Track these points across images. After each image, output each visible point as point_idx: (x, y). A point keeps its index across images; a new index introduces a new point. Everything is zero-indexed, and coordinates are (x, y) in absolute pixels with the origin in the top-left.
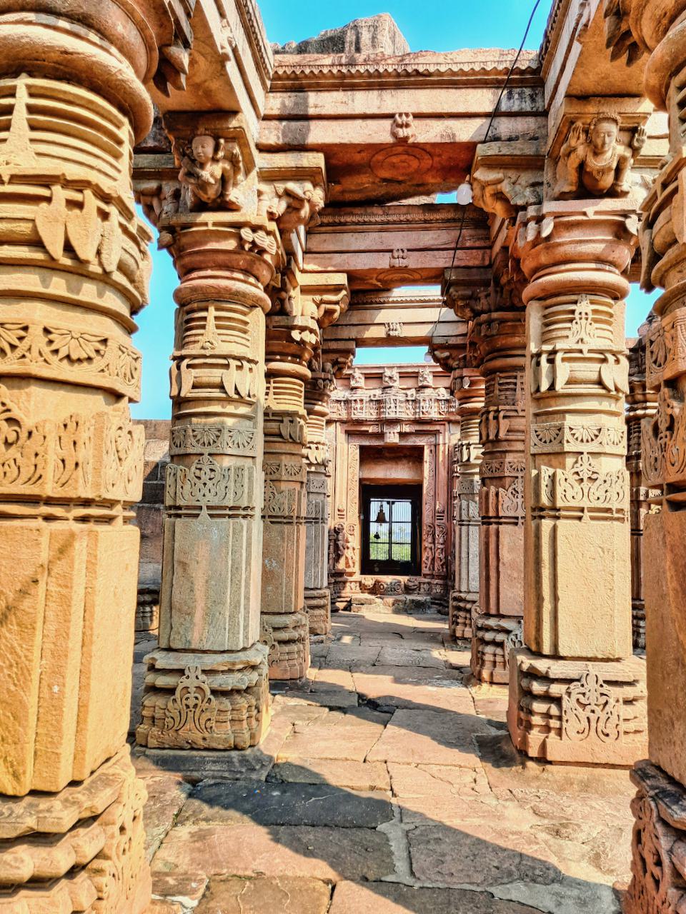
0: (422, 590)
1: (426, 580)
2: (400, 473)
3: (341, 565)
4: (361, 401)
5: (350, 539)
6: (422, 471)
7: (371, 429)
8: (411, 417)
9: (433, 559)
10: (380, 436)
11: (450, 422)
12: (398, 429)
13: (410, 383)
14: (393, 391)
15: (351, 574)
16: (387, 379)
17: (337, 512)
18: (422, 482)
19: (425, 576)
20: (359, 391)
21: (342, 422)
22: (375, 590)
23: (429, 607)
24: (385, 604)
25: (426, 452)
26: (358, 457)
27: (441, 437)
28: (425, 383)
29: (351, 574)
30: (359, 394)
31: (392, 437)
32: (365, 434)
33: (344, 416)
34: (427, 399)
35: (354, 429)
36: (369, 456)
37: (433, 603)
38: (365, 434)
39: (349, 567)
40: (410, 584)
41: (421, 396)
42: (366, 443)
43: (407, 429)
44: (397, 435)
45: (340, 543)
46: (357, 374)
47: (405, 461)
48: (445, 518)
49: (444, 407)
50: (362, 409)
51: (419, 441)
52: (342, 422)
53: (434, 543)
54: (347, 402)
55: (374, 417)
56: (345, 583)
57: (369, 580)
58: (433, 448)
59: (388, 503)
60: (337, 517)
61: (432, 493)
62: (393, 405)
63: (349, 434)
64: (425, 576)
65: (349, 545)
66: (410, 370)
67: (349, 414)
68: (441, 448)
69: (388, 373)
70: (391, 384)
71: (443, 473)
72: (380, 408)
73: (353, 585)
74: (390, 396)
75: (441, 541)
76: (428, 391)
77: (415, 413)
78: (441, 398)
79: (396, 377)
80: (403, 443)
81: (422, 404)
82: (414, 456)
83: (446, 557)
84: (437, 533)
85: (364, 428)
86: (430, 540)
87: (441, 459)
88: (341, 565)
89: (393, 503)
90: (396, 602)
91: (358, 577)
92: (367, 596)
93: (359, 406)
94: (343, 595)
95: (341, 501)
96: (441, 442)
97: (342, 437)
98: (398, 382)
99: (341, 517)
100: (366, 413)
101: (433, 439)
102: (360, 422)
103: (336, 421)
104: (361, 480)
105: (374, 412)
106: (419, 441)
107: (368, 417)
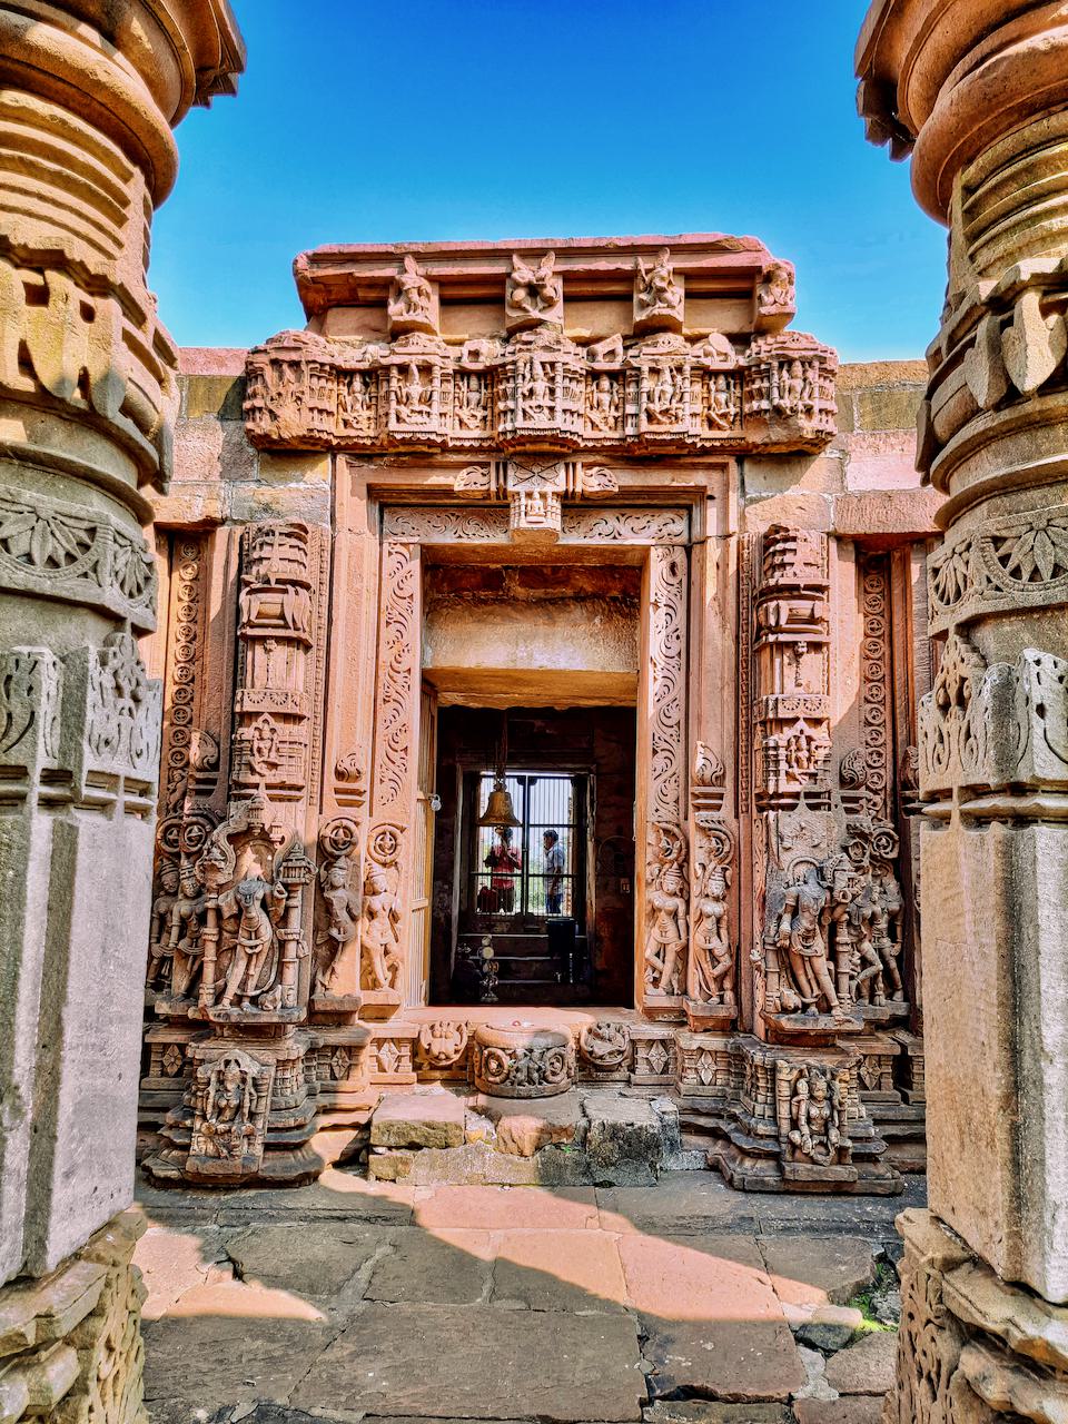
0: (642, 1068)
1: (659, 1032)
2: (552, 654)
3: (344, 983)
4: (426, 370)
5: (382, 878)
6: (635, 649)
7: (459, 481)
8: (609, 434)
9: (683, 953)
10: (495, 508)
11: (744, 454)
12: (558, 481)
13: (603, 321)
14: (546, 336)
15: (382, 1013)
16: (520, 294)
17: (331, 781)
18: (634, 686)
19: (651, 1014)
20: (419, 341)
21: (360, 454)
22: (469, 1072)
23: (674, 1146)
24: (507, 1144)
25: (657, 570)
26: (414, 586)
27: (712, 511)
28: (659, 309)
29: (382, 1013)
30: (415, 349)
31: (536, 507)
32: (439, 503)
33: (364, 429)
34: (666, 364)
35: (398, 475)
36: (455, 585)
37: (686, 1127)
38: (439, 503)
39: (375, 985)
40: (601, 1048)
41: (643, 356)
42: (446, 535)
43: (590, 481)
44: (556, 505)
45: (338, 898)
46: (412, 276)
47: (577, 613)
48: (728, 802)
49: (724, 399)
50: (428, 400)
51: (632, 533)
52: (360, 454)
53: (684, 892)
54: (374, 375)
55: (474, 432)
56: (352, 1050)
57: (450, 1029)
58: (679, 556)
59: (521, 780)
60: (330, 797)
61: (677, 715)
62: (541, 386)
63: (384, 501)
64: (651, 1014)
65: (376, 903)
66: (603, 265)
67: (380, 420)
68: (713, 551)
69: (524, 272)
70: (535, 314)
71: (718, 639)
72: (494, 399)
73: (387, 1054)
74: (531, 355)
75: (716, 887)
76: (669, 342)
77: (621, 421)
78: (715, 363)
79: (554, 288)
80: (574, 539)
81: (647, 384)
82: (613, 589)
83: (736, 952)
84: (698, 856)
85: (436, 479)
86: (671, 883)
87: (711, 590)
88: (344, 983)
89: (533, 781)
90: (549, 1136)
91: (412, 1013)
92: (441, 1105)
93: (416, 388)
94: (343, 1100)
95: (350, 740)
96: (712, 529)
97: (356, 510)
98: (555, 315)
99: (350, 798)
100: (449, 418)
101: (680, 526)
102: (421, 453)
103: (332, 450)
104: (430, 683)
105: (473, 415)
106: (632, 533)
107: (450, 431)
